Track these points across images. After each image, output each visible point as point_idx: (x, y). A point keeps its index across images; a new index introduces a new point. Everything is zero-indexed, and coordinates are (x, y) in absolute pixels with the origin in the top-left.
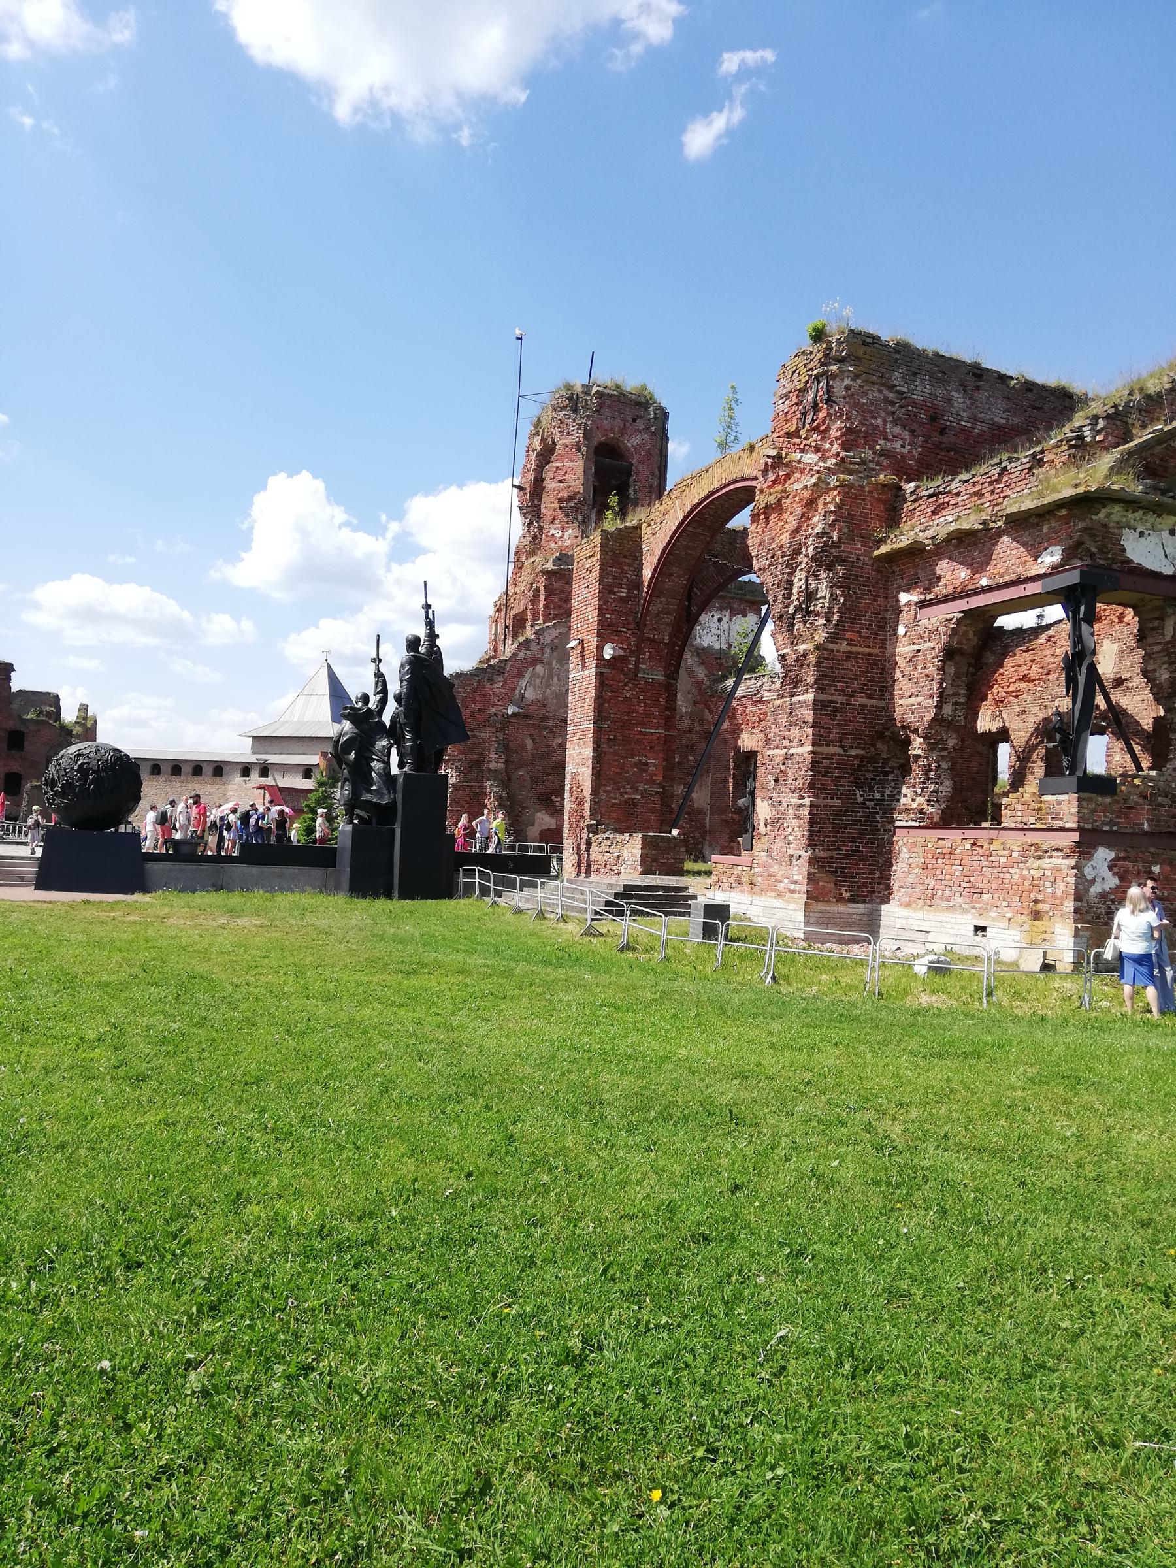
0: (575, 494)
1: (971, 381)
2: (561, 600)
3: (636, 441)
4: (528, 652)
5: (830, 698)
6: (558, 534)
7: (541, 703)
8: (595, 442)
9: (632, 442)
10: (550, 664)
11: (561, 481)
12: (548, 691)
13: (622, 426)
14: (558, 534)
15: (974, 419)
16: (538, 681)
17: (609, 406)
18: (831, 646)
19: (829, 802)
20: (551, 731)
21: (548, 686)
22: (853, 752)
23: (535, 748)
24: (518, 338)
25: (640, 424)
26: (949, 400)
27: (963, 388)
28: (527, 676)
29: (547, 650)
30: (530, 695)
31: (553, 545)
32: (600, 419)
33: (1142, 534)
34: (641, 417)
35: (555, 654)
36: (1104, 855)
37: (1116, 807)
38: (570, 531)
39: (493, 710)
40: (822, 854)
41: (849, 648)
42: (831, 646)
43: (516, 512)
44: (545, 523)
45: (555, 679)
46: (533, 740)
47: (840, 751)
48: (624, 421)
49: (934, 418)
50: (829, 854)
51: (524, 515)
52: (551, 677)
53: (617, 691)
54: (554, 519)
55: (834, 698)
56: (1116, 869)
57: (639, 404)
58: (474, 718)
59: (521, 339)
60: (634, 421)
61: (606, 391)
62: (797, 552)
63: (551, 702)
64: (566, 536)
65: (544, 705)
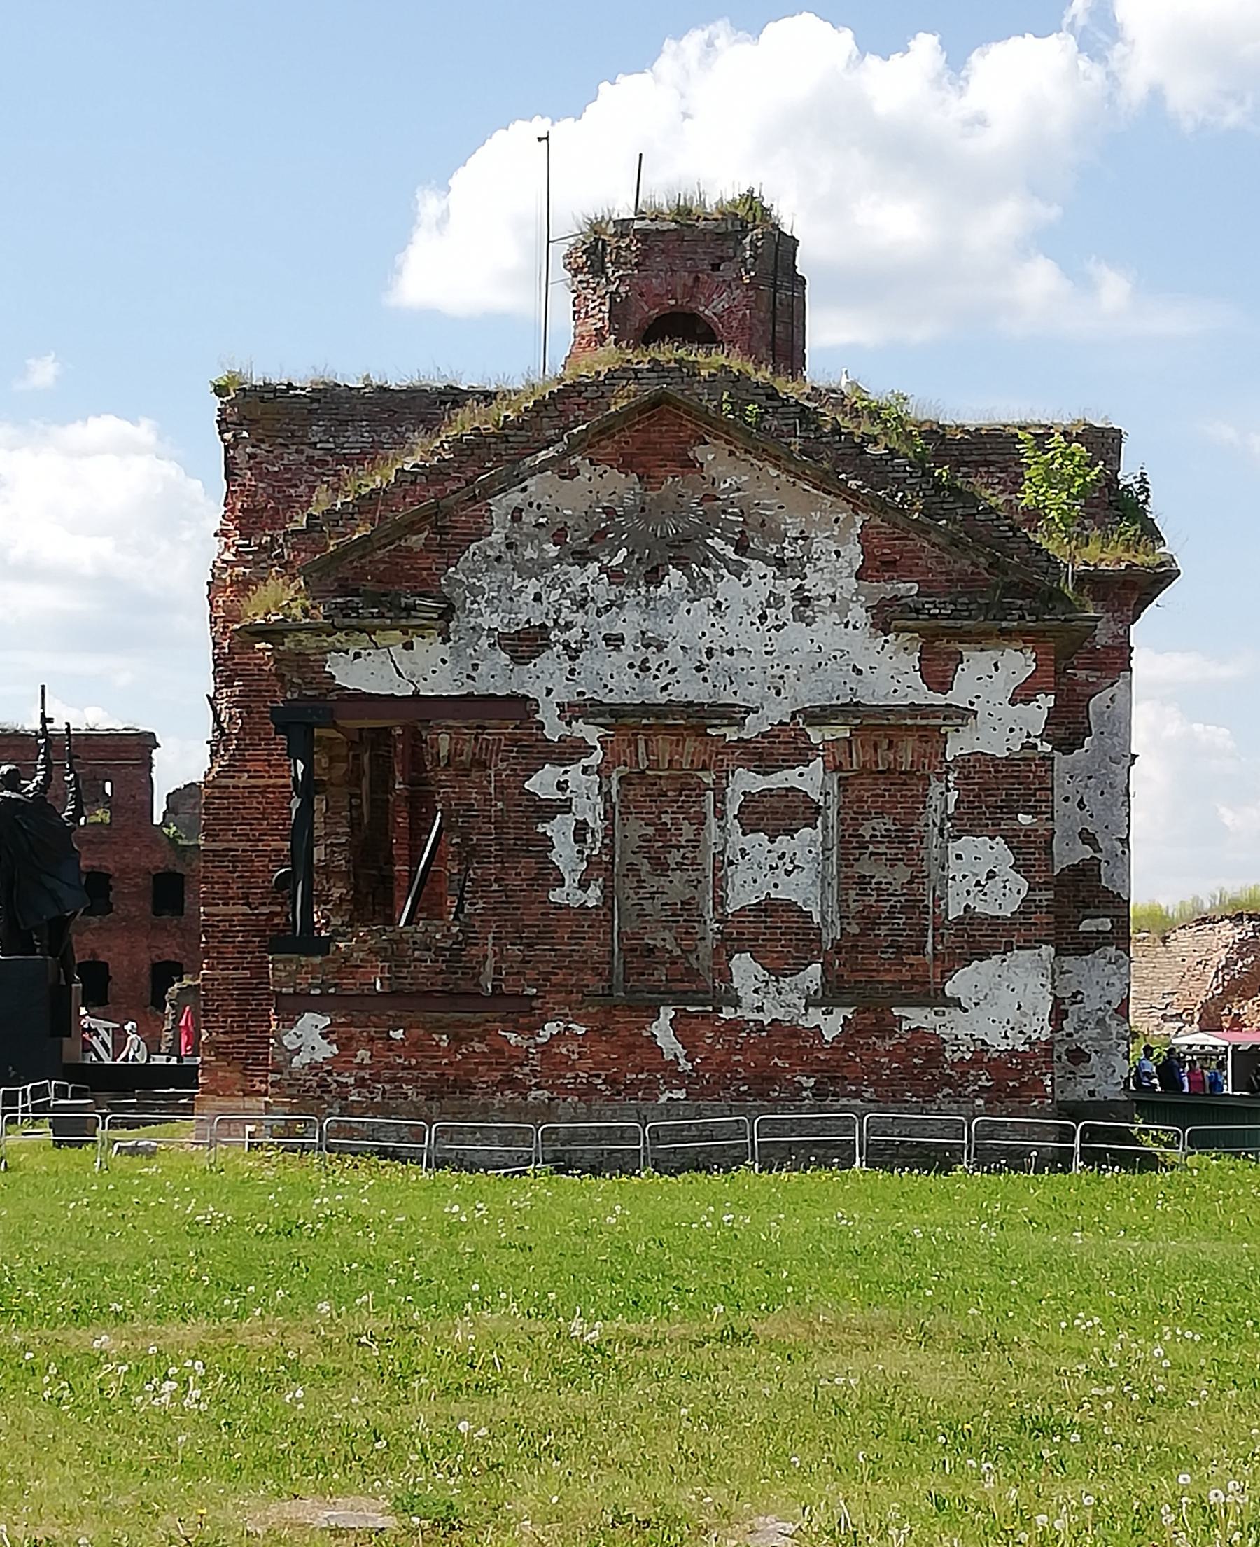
3: (720, 304)
5: (226, 845)
13: (690, 283)
17: (663, 251)
18: (224, 782)
19: (236, 974)
22: (265, 910)
24: (540, 139)
32: (646, 277)
33: (357, 656)
36: (312, 1024)
37: (332, 967)
40: (222, 1038)
41: (253, 781)
42: (224, 782)
47: (247, 910)
50: (236, 1037)
55: (232, 845)
56: (333, 1037)
57: (721, 236)
59: (547, 138)
60: (715, 267)
61: (658, 225)
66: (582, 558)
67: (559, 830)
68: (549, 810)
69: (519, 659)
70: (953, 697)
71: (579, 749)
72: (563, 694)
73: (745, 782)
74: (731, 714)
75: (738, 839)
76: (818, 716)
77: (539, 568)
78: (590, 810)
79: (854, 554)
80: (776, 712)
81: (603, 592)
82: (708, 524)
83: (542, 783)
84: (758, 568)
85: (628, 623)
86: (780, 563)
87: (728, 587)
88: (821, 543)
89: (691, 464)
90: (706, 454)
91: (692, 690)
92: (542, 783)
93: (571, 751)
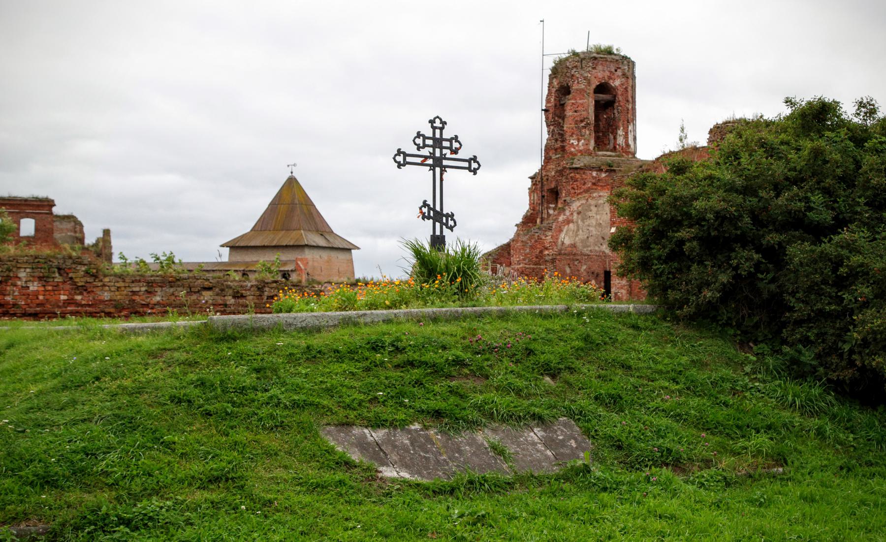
0: (584, 119)
2: (581, 184)
4: (565, 217)
6: (575, 143)
7: (574, 246)
8: (594, 86)
9: (616, 83)
10: (577, 222)
11: (576, 112)
12: (577, 238)
14: (575, 143)
16: (571, 233)
17: (602, 64)
20: (580, 262)
21: (577, 235)
23: (572, 273)
25: (619, 72)
28: (565, 230)
29: (575, 215)
30: (567, 241)
31: (573, 149)
34: (620, 68)
35: (580, 216)
38: (583, 141)
39: (546, 252)
43: (544, 124)
44: (567, 136)
45: (581, 231)
46: (570, 267)
48: (611, 72)
51: (548, 126)
52: (578, 230)
54: (573, 134)
58: (537, 258)
60: (616, 71)
63: (579, 245)
64: (581, 143)
65: (575, 247)
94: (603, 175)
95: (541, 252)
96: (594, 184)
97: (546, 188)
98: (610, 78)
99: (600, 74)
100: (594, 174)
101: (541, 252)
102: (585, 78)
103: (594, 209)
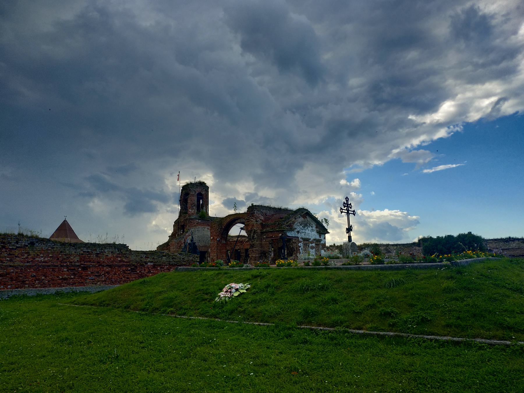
1: (270, 209)
8: (197, 193)
14: (191, 211)
15: (270, 214)
25: (204, 190)
26: (267, 212)
27: (269, 210)
49: (266, 214)
53: (219, 245)
62: (252, 231)
66: (301, 225)
67: (300, 248)
68: (300, 247)
69: (298, 234)
70: (321, 239)
71: (301, 242)
72: (300, 237)
73: (311, 245)
74: (310, 239)
75: (311, 250)
76: (314, 240)
77: (298, 226)
78: (302, 247)
79: (315, 227)
80: (312, 239)
81: (302, 228)
82: (307, 223)
83: (299, 244)
84: (310, 227)
85: (304, 231)
86: (311, 226)
87: (309, 228)
88: (314, 225)
89: (306, 218)
90: (307, 217)
91: (307, 237)
92: (299, 244)
93: (301, 242)
94: (200, 221)
95: (181, 245)
96: (197, 224)
97: (180, 225)
98: (201, 191)
99: (198, 190)
100: (197, 221)
101: (181, 245)
102: (194, 191)
103: (197, 232)
